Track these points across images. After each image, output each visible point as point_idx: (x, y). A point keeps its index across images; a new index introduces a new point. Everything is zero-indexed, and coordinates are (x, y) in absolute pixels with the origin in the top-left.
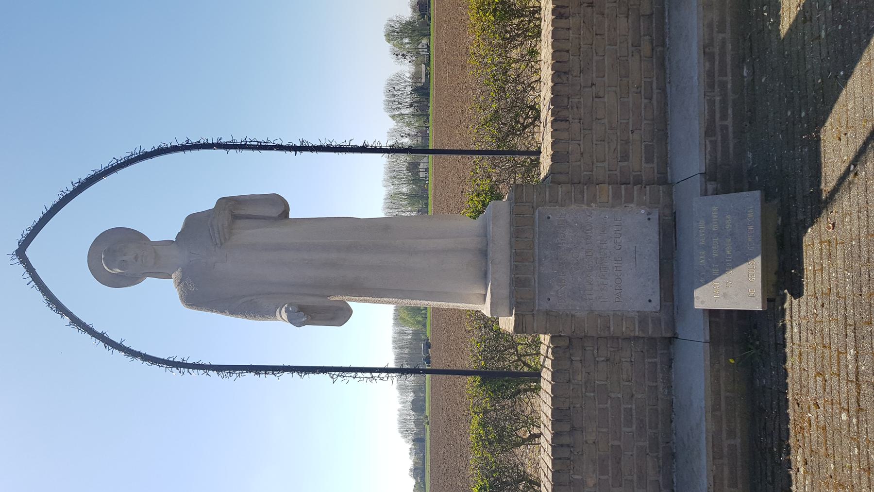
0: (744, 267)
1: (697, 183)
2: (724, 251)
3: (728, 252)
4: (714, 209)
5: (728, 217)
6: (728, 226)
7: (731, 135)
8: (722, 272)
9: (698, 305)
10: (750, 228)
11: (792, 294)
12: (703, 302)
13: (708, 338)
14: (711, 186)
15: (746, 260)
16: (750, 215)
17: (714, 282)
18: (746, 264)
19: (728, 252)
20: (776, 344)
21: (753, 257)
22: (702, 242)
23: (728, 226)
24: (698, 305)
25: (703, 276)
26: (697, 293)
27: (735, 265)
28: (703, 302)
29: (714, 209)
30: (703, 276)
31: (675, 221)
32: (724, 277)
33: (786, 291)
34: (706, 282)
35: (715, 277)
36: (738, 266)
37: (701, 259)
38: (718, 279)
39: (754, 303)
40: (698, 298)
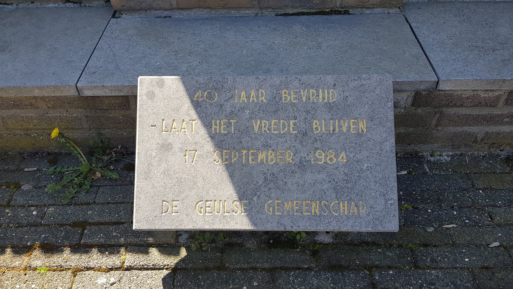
0: (228, 191)
1: (419, 76)
2: (266, 146)
3: (261, 156)
4: (362, 126)
5: (343, 157)
6: (321, 157)
7: (493, 129)
8: (220, 142)
9: (145, 84)
10: (315, 208)
11: (175, 270)
12: (151, 95)
13: (88, 93)
14: (406, 98)
15: (242, 196)
16: (344, 208)
17: (197, 124)
18: (235, 196)
19: (261, 156)
20: (83, 225)
21: (250, 211)
22: (288, 96)
23: (321, 157)
24: (145, 84)
25: (210, 97)
26: (172, 83)
27: (231, 169)
28: (151, 95)
29: (362, 126)
30: (210, 97)
31: (334, 12)
32: (208, 146)
33: (184, 253)
34: (196, 105)
35: (207, 125)
36: (232, 176)
37: (249, 93)
38: (203, 131)
39: (146, 214)
40: (161, 84)
